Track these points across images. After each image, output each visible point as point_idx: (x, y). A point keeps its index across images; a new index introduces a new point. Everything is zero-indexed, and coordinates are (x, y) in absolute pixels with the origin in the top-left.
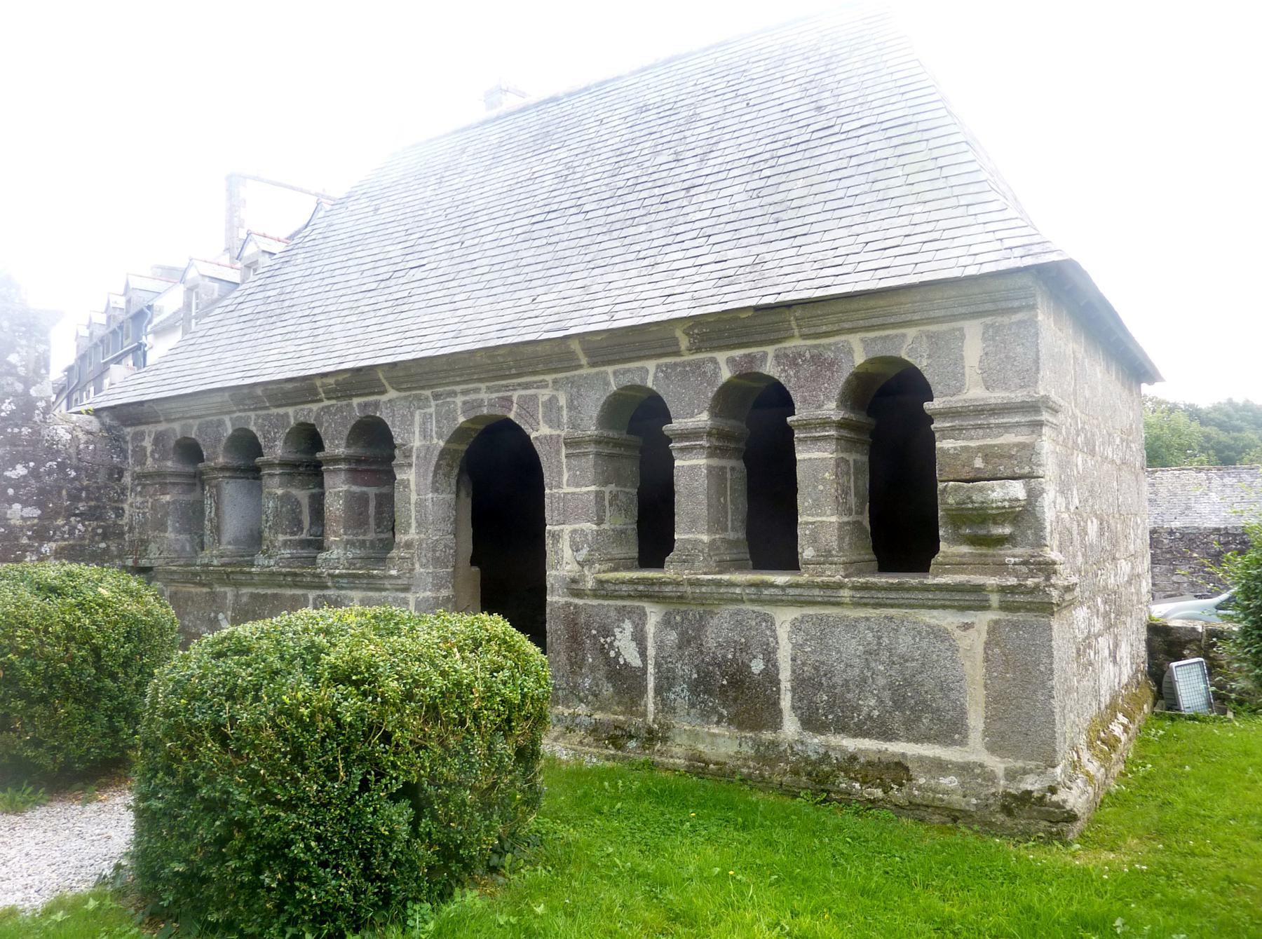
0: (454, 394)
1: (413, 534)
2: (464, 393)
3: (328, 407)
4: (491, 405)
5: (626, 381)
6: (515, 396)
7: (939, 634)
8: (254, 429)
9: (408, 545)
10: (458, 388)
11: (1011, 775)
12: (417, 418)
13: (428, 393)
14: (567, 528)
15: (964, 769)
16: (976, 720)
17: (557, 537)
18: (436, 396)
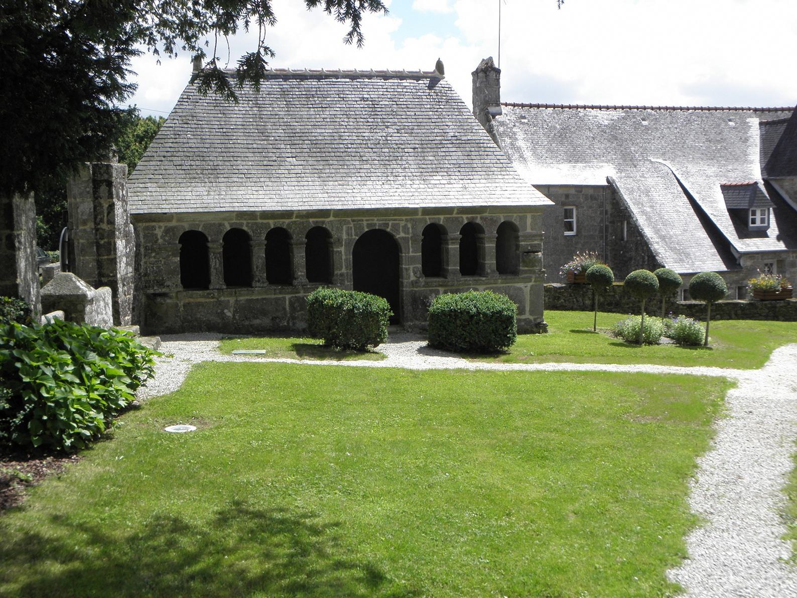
0: (363, 220)
1: (344, 270)
2: (367, 220)
3: (295, 222)
4: (380, 225)
5: (433, 221)
6: (390, 223)
7: (520, 289)
8: (245, 228)
9: (342, 275)
10: (364, 219)
11: (535, 319)
12: (344, 227)
13: (350, 219)
14: (411, 267)
15: (525, 320)
16: (527, 309)
17: (407, 270)
18: (353, 221)
